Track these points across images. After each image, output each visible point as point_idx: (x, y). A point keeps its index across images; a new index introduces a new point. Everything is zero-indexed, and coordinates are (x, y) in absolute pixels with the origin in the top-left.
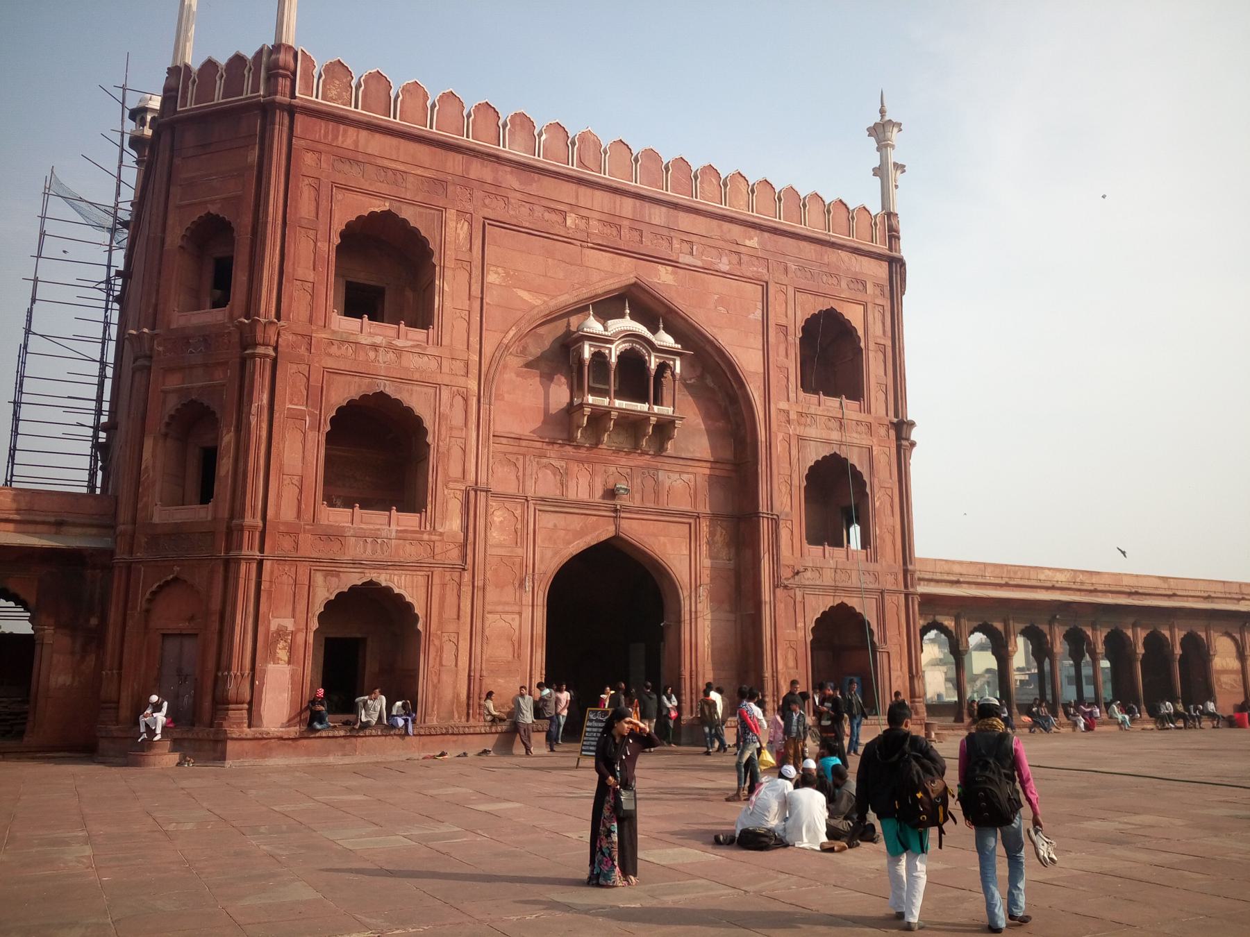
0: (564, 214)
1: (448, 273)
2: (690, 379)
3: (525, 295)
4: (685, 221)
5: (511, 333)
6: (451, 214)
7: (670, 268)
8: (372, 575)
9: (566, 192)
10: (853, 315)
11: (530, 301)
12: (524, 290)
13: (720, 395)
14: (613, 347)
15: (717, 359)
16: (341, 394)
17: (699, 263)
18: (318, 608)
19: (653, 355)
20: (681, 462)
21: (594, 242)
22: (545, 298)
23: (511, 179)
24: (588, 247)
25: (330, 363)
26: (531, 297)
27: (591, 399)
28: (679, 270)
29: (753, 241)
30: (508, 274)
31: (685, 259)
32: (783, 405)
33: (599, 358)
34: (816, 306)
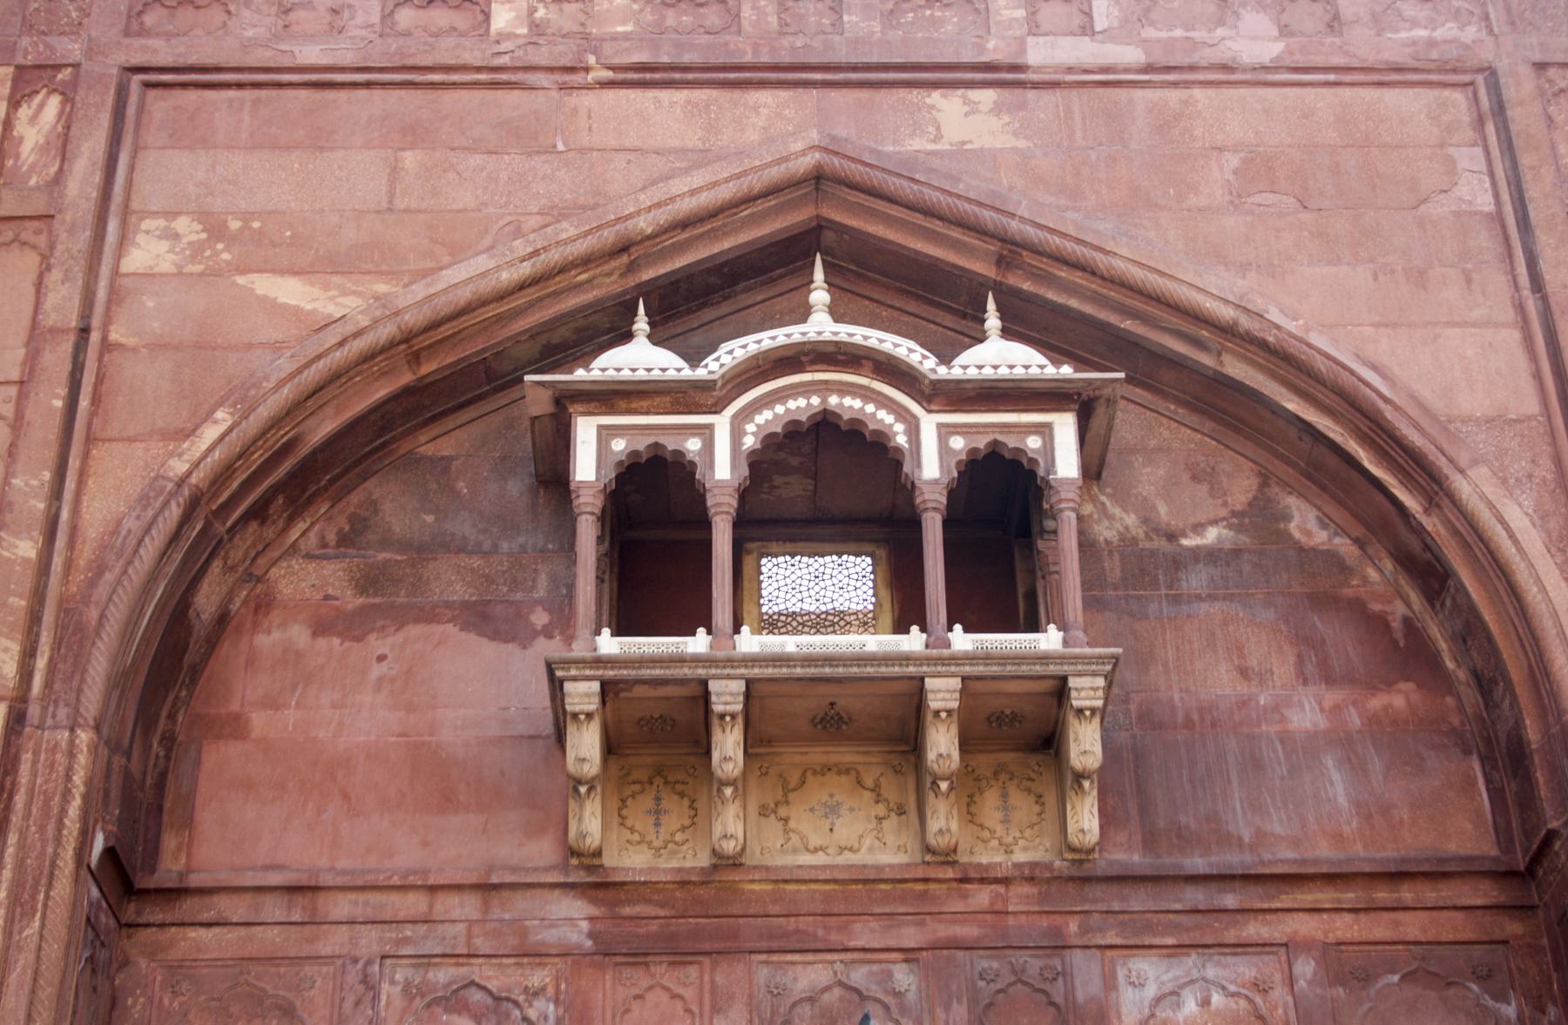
2: (1198, 528)
3: (290, 291)
5: (210, 433)
7: (987, 96)
11: (309, 307)
12: (282, 272)
13: (1373, 574)
14: (721, 423)
15: (1293, 405)
17: (1131, 55)
19: (929, 423)
20: (1195, 896)
21: (616, 61)
22: (382, 288)
24: (588, 87)
26: (317, 292)
28: (1031, 95)
30: (216, 230)
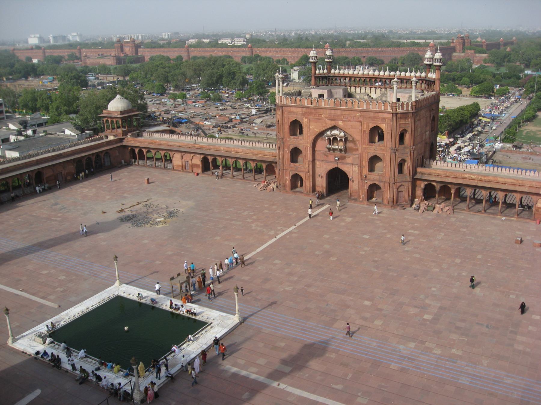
0: (322, 115)
1: (304, 128)
4: (345, 113)
6: (304, 118)
8: (297, 173)
9: (322, 111)
10: (383, 126)
16: (291, 147)
18: (291, 176)
23: (313, 111)
25: (289, 143)
27: (328, 146)
29: (358, 114)
31: (344, 119)
32: (364, 146)
33: (329, 139)
34: (372, 125)
